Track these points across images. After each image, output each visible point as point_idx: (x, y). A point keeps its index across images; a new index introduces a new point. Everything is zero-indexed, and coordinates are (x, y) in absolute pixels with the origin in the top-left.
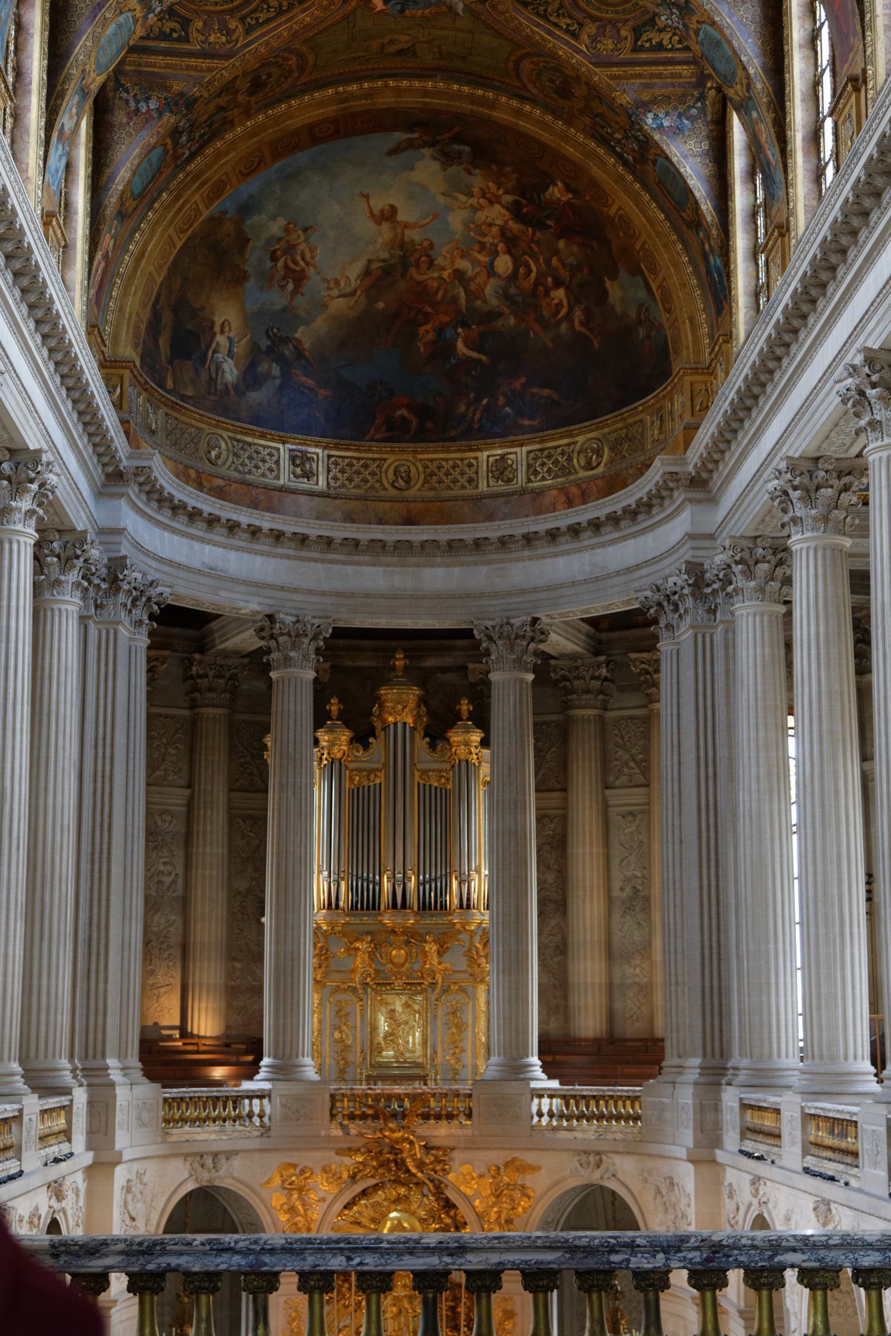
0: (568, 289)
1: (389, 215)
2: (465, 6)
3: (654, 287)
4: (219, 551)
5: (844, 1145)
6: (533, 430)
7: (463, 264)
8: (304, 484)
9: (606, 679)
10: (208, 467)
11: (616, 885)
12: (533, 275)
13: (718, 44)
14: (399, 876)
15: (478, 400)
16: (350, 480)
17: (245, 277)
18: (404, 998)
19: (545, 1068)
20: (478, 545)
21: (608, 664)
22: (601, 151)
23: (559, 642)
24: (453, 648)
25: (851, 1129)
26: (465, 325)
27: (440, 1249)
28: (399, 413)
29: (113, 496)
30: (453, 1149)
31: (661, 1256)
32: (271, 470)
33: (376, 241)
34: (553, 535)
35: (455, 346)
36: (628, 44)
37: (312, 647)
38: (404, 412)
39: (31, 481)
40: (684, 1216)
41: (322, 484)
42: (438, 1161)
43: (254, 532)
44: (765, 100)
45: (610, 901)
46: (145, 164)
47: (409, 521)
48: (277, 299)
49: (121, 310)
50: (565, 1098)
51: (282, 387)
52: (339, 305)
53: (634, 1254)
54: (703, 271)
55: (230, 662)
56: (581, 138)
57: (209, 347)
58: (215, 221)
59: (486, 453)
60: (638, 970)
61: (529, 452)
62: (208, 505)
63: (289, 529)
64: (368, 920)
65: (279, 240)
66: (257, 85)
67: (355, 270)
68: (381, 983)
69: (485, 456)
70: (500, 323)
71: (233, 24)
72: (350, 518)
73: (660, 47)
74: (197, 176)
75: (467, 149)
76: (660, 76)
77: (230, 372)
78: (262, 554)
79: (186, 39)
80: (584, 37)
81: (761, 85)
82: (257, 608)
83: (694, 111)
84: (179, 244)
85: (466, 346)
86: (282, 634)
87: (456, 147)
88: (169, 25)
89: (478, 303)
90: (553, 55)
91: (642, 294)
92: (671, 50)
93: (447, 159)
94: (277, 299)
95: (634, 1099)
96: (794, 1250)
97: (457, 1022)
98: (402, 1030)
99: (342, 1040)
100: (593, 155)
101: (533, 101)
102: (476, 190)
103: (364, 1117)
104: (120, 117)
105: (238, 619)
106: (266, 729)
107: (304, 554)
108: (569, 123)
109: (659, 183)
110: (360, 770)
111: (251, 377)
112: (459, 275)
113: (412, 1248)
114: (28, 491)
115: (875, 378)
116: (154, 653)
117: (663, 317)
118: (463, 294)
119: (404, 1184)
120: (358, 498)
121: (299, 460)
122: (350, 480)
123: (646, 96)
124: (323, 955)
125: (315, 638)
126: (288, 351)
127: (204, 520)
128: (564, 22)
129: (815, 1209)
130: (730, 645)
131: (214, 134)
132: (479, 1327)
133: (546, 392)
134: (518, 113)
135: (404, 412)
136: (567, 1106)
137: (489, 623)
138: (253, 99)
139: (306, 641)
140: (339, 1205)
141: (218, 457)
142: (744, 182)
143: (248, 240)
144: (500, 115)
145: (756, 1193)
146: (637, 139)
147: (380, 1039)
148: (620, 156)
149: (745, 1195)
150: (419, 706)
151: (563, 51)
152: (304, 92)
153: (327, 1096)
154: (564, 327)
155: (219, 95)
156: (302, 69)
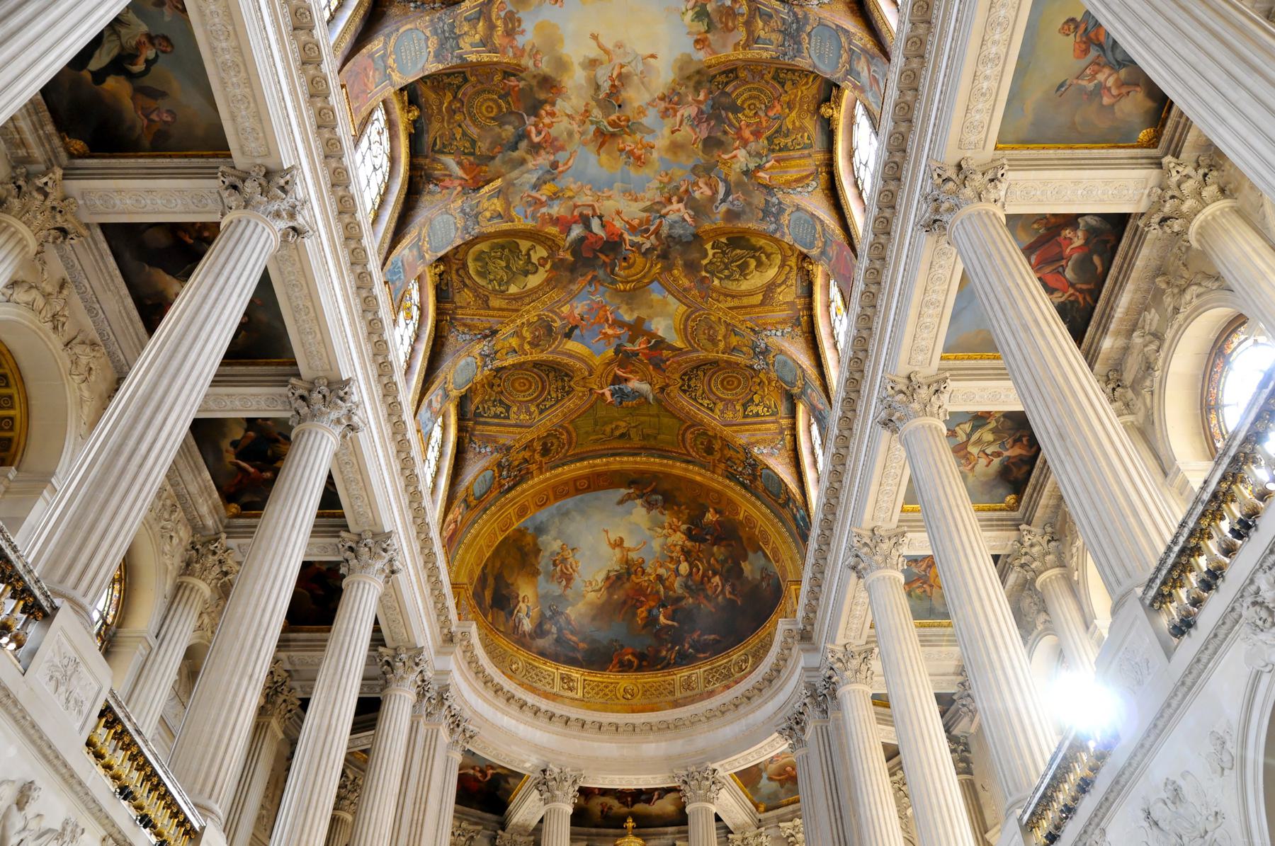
0: (721, 575)
1: (619, 543)
2: (656, 399)
6: (706, 658)
7: (662, 571)
13: (785, 363)
15: (673, 648)
22: (732, 484)
24: (666, 834)
26: (664, 606)
29: (445, 654)
33: (611, 561)
35: (656, 619)
36: (741, 414)
37: (571, 790)
38: (630, 657)
39: (385, 550)
41: (580, 695)
43: (536, 712)
46: (481, 477)
48: (556, 589)
49: (462, 560)
51: (558, 641)
52: (592, 596)
56: (720, 479)
58: (521, 532)
62: (508, 685)
66: (546, 451)
67: (601, 576)
70: (683, 603)
71: (533, 408)
73: (757, 415)
77: (527, 625)
79: (508, 418)
80: (717, 411)
81: (812, 372)
84: (501, 539)
87: (654, 497)
88: (500, 409)
90: (701, 423)
91: (763, 561)
93: (650, 506)
100: (728, 486)
104: (470, 455)
107: (567, 731)
108: (713, 472)
109: (766, 489)
111: (539, 631)
112: (659, 577)
114: (380, 556)
115: (897, 388)
116: (471, 827)
117: (775, 567)
123: (753, 440)
126: (562, 620)
128: (706, 402)
130: (841, 727)
133: (712, 637)
134: (686, 470)
135: (630, 657)
137: (685, 773)
138: (544, 460)
144: (675, 471)
146: (750, 465)
151: (706, 419)
152: (572, 462)
154: (720, 597)
155: (525, 449)
156: (570, 444)
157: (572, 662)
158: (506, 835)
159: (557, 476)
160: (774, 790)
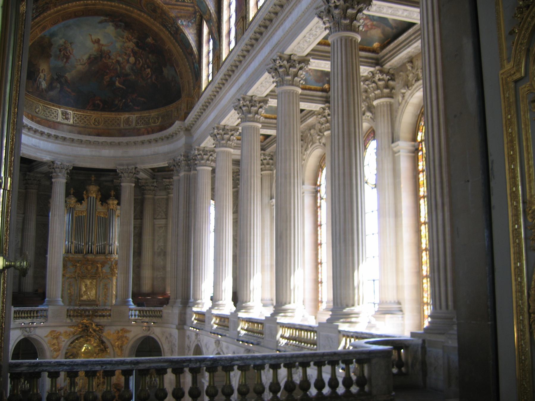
1: (97, 42)
3: (177, 71)
4: (38, 140)
5: (224, 324)
6: (138, 110)
7: (120, 59)
8: (66, 122)
9: (156, 187)
10: (35, 114)
11: (156, 248)
12: (141, 64)
14: (90, 243)
16: (80, 121)
17: (51, 56)
18: (90, 281)
19: (133, 302)
20: (119, 144)
21: (156, 182)
22: (164, 29)
23: (142, 175)
25: (227, 320)
26: (119, 77)
27: (131, 363)
28: (97, 102)
30: (105, 326)
31: (198, 364)
32: (55, 116)
33: (93, 49)
34: (143, 143)
35: (114, 83)
38: (98, 102)
40: (174, 345)
42: (100, 329)
43: (49, 135)
44: (215, 20)
45: (154, 253)
47: (98, 135)
48: (60, 64)
50: (140, 311)
52: (80, 67)
53: (190, 363)
54: (193, 68)
55: (39, 175)
56: (158, 25)
57: (37, 76)
59: (123, 116)
60: (161, 273)
61: (136, 117)
63: (60, 134)
64: (80, 256)
65: (62, 46)
67: (85, 57)
68: (83, 277)
69: (124, 116)
72: (80, 133)
74: (38, 23)
75: (123, 24)
76: (184, 10)
77: (44, 85)
78: (52, 142)
81: (214, 15)
82: (49, 159)
83: (193, 21)
85: (119, 83)
86: (56, 168)
87: (120, 23)
89: (123, 71)
92: (188, 2)
93: (117, 26)
94: (60, 64)
95: (160, 311)
96: (237, 360)
97: (106, 287)
98: (89, 291)
99: (70, 293)
101: (145, 13)
102: (125, 37)
103: (77, 316)
105: (42, 162)
106: (49, 197)
107: (65, 143)
108: (155, 20)
110: (79, 211)
111: (51, 87)
112: (118, 62)
113: (122, 363)
118: (119, 68)
119: (90, 336)
120: (83, 127)
121: (65, 114)
122: (80, 121)
123: (179, 15)
124: (65, 266)
125: (67, 169)
127: (33, 131)
129: (215, 342)
131: (44, 11)
132: (142, 385)
133: (143, 99)
135: (98, 102)
136: (140, 313)
139: (64, 170)
140: (69, 343)
141: (38, 111)
142: (206, 43)
143: (52, 45)
144: (134, 15)
145: (196, 338)
147: (82, 292)
148: (170, 32)
149: (193, 337)
150: (98, 192)
153: (66, 310)
154: (149, 80)
157: (67, 105)
158: (32, 174)
159: (65, 9)
160: (162, 175)
